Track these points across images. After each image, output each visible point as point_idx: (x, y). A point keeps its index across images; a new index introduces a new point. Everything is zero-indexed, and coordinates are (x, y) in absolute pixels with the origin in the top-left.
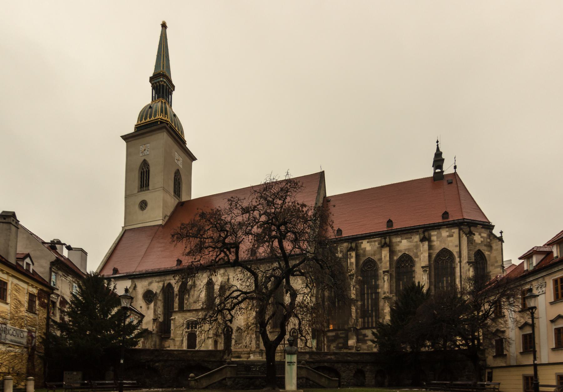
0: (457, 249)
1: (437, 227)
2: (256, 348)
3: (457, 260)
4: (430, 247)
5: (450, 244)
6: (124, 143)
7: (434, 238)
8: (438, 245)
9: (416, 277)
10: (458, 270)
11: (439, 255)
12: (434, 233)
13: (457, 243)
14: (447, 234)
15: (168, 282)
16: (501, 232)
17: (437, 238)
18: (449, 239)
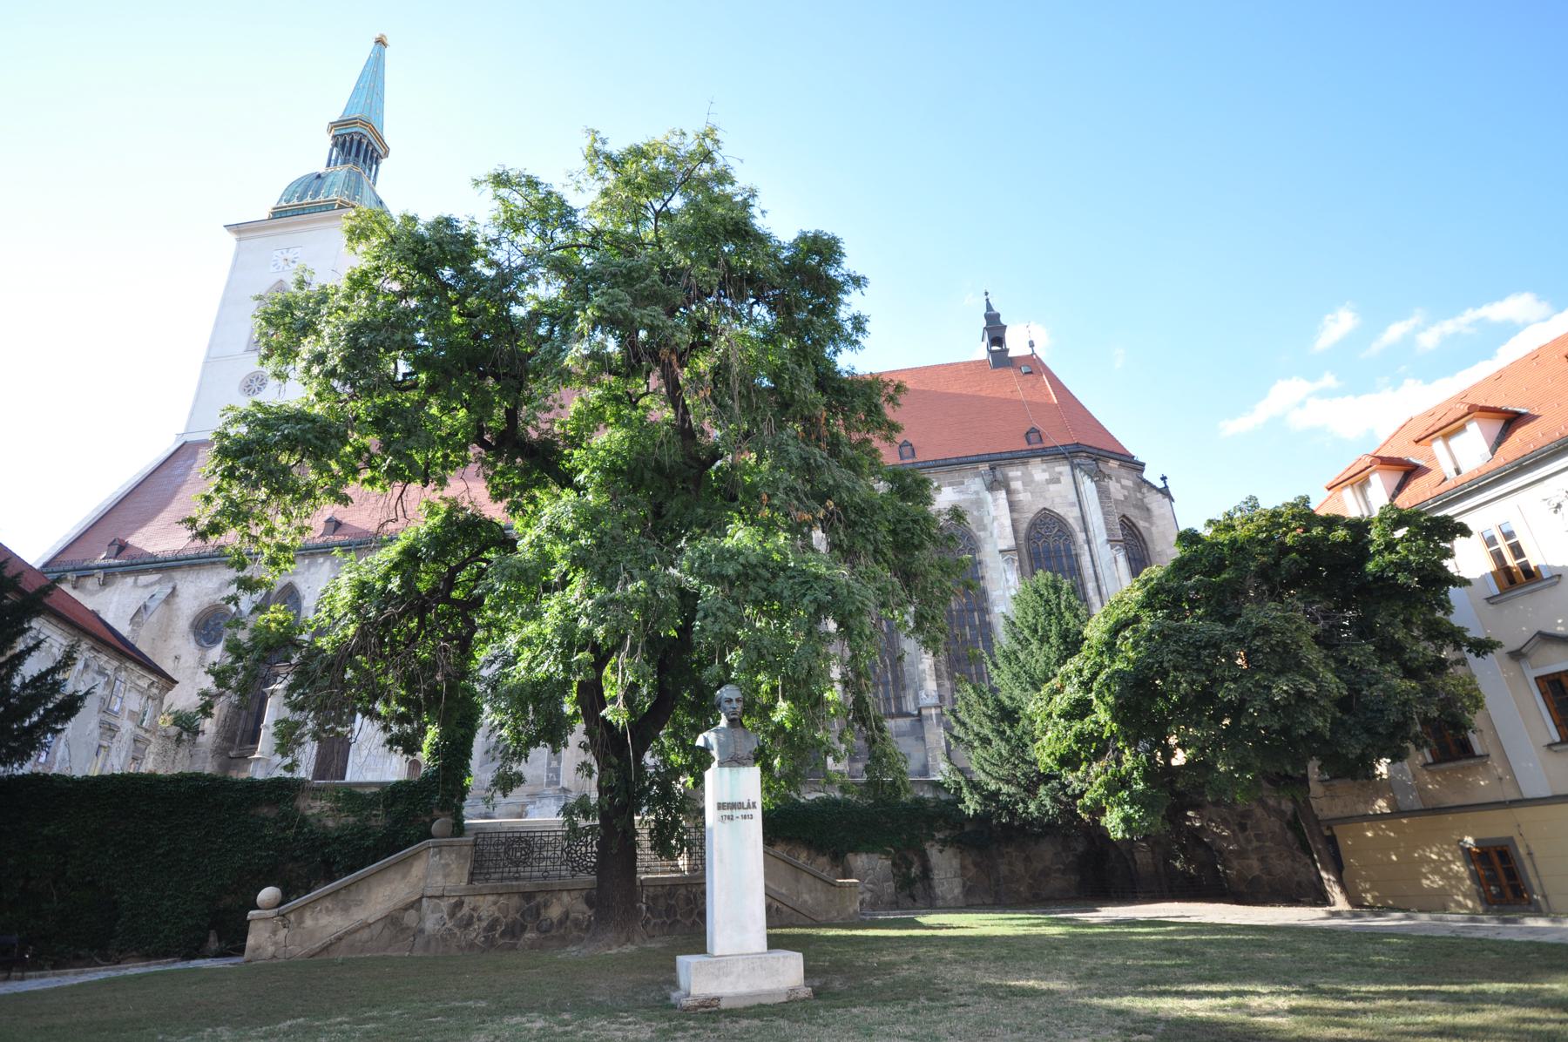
0: (1076, 512)
1: (1020, 458)
2: (549, 784)
3: (1081, 537)
4: (1013, 506)
5: (1057, 500)
6: (231, 239)
7: (1016, 485)
8: (1031, 503)
9: (987, 576)
10: (1085, 560)
11: (1033, 525)
12: (1014, 473)
13: (1073, 497)
14: (1046, 476)
15: (287, 580)
16: (1164, 479)
17: (1024, 484)
18: (1052, 487)
